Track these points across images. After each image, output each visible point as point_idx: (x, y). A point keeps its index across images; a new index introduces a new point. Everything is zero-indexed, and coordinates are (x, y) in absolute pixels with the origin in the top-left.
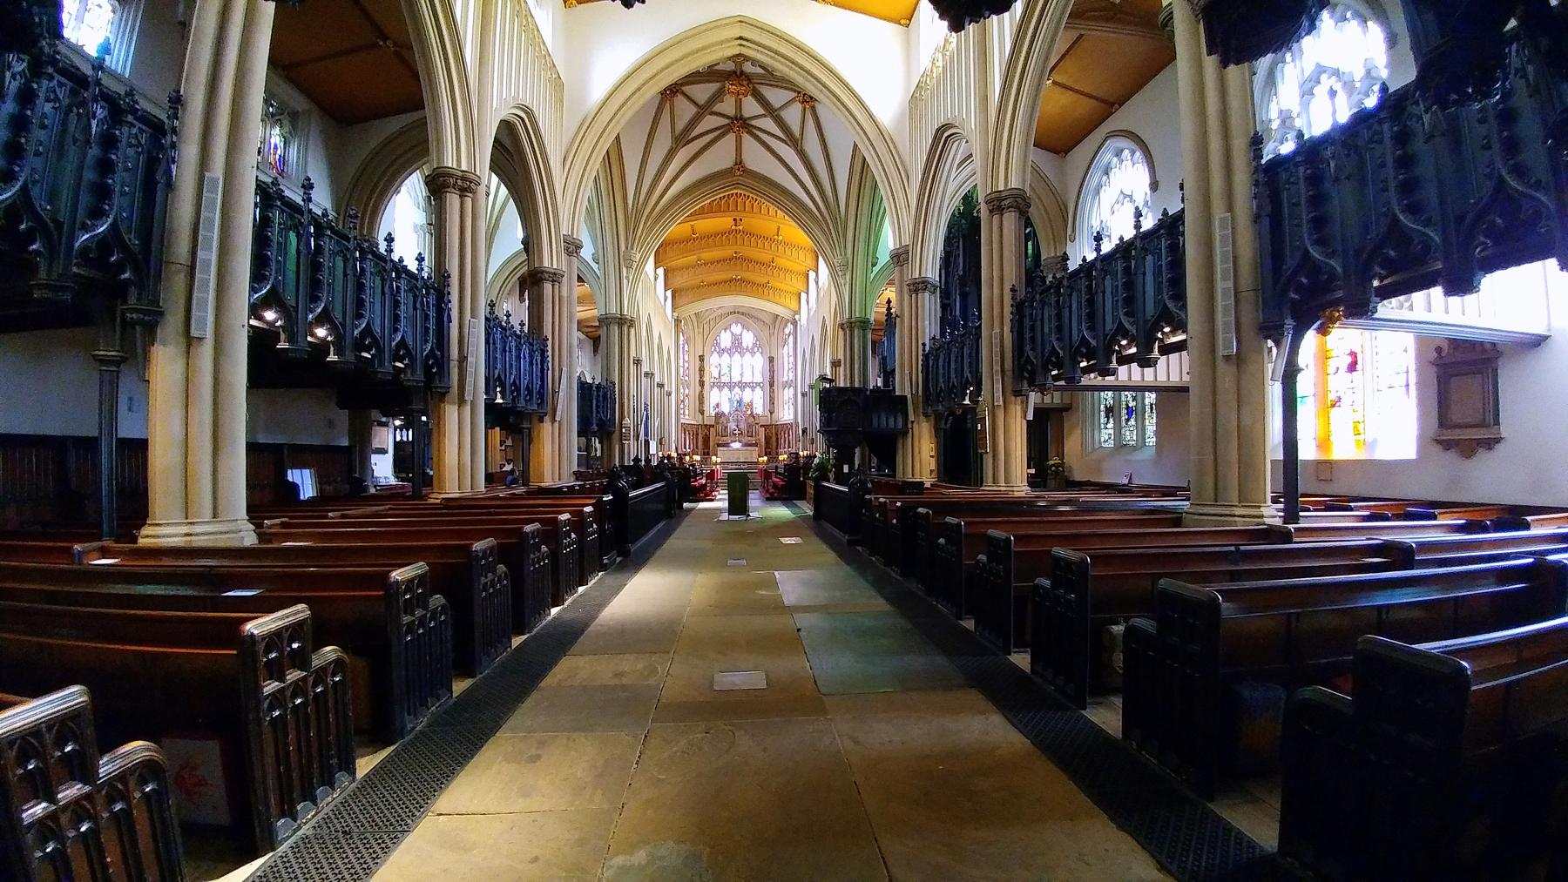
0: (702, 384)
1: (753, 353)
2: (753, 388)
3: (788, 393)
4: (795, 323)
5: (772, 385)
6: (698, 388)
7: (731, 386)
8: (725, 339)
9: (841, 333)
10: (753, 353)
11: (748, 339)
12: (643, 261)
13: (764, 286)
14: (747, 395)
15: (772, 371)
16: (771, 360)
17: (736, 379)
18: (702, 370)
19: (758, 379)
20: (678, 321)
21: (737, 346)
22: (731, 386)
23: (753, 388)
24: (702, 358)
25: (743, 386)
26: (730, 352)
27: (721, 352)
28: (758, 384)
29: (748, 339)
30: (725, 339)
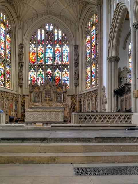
0: (21, 65)
1: (62, 46)
2: (62, 70)
5: (76, 65)
6: (18, 69)
7: (44, 66)
8: (41, 35)
10: (62, 46)
15: (77, 55)
16: (76, 47)
17: (50, 62)
18: (21, 55)
19: (65, 61)
21: (49, 39)
22: (44, 66)
23: (62, 70)
24: (21, 46)
25: (54, 67)
26: (44, 43)
27: (38, 44)
28: (66, 66)
29: (58, 34)
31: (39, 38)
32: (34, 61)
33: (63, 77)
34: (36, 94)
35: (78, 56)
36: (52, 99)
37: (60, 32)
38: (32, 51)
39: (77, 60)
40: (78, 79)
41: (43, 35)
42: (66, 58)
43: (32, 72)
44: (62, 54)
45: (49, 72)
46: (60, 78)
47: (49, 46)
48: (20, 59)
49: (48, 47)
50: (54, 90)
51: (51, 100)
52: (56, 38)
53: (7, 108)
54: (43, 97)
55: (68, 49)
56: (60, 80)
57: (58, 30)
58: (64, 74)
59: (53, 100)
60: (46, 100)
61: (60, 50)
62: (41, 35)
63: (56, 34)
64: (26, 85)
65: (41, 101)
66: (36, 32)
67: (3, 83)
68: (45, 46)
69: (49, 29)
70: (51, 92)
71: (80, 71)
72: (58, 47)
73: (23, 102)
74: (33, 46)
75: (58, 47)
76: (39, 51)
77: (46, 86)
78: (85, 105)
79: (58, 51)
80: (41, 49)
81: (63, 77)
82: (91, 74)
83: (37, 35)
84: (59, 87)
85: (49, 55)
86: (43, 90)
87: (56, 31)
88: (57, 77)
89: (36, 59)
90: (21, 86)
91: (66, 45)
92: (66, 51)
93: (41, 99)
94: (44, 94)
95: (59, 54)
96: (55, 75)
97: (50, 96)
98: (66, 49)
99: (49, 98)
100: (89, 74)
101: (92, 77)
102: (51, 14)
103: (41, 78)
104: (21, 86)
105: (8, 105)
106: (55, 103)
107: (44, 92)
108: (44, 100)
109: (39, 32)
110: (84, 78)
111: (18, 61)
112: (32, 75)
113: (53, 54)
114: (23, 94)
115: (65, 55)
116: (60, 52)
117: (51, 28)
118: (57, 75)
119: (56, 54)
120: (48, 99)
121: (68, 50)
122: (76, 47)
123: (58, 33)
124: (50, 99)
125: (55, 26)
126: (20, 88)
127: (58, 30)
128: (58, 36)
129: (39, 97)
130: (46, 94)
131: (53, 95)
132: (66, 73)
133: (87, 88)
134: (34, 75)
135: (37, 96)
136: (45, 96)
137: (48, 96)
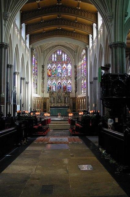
0: (43, 79)
2: (67, 80)
3: (84, 82)
4: (86, 50)
6: (41, 81)
8: (54, 57)
9: (110, 50)
10: (67, 64)
11: (65, 57)
12: (14, 16)
13: (72, 32)
14: (64, 83)
16: (75, 67)
20: (32, 50)
21: (60, 60)
24: (43, 67)
27: (52, 63)
28: (70, 77)
29: (65, 57)
30: (54, 57)
31: (53, 60)
32: (50, 75)
35: (76, 72)
37: (66, 55)
38: (49, 68)
39: (76, 75)
40: (77, 87)
41: (56, 58)
42: (69, 73)
43: (49, 82)
44: (67, 70)
45: (59, 82)
47: (59, 65)
48: (43, 75)
49: (59, 65)
50: (63, 96)
52: (63, 60)
55: (70, 67)
56: (65, 88)
57: (64, 55)
61: (66, 68)
62: (54, 58)
63: (63, 57)
64: (46, 89)
66: (52, 56)
68: (57, 65)
69: (59, 53)
71: (78, 82)
72: (65, 65)
74: (50, 65)
75: (65, 65)
76: (53, 68)
79: (64, 68)
80: (54, 67)
82: (84, 85)
83: (52, 58)
85: (59, 71)
87: (63, 55)
89: (51, 74)
91: (69, 64)
92: (69, 68)
95: (65, 70)
98: (69, 66)
100: (83, 84)
102: (60, 45)
104: (43, 92)
106: (63, 104)
109: (53, 55)
110: (80, 87)
111: (41, 76)
113: (62, 70)
115: (69, 71)
116: (66, 69)
117: (61, 53)
119: (64, 70)
121: (71, 67)
122: (75, 67)
123: (65, 56)
125: (62, 52)
127: (64, 55)
128: (64, 58)
132: (69, 83)
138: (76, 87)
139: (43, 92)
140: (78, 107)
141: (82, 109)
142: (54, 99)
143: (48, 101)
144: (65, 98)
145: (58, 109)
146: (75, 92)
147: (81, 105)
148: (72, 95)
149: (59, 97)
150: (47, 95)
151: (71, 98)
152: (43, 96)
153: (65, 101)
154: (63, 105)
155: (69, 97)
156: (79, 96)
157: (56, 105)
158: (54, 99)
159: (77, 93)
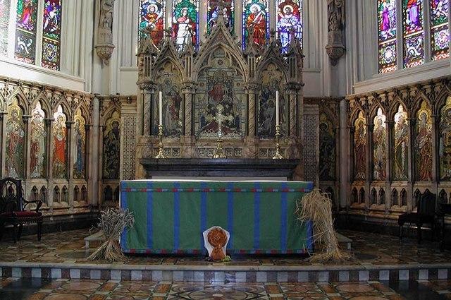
33: (280, 18)
34: (169, 94)
36: (237, 119)
40: (342, 27)
46: (264, 22)
51: (233, 126)
53: (40, 160)
54: (197, 112)
58: (281, 6)
59: (243, 126)
60: (214, 126)
65: (188, 127)
67: (29, 45)
70: (235, 87)
73: (109, 129)
77: (214, 57)
78: (379, 148)
81: (280, 18)
84: (271, 62)
86: (200, 75)
88: (252, 16)
90: (103, 55)
93: (188, 120)
94: (203, 97)
96: (248, 7)
97: (231, 106)
99: (224, 113)
101: (408, 21)
103: (188, 21)
105: (47, 147)
106: (250, 140)
107: (205, 87)
108: (203, 122)
112: (152, 10)
114: (113, 93)
118: (252, 10)
120: (220, 118)
124: (231, 118)
126: (97, 66)
129: (181, 112)
130: (214, 94)
131: (244, 102)
133: (381, 66)
134: (160, 7)
135: (170, 104)
136: (210, 107)
137: (220, 108)
138: (339, 25)
139: (104, 58)
140: (355, 169)
141: (400, 186)
142: (178, 101)
143: (130, 121)
144: (265, 96)
145: (204, 189)
146: (334, 60)
147: (380, 153)
148: (317, 80)
149: (219, 91)
150: (125, 78)
151: (309, 101)
152: (106, 79)
153: (260, 117)
154: (247, 152)
155: (295, 87)
156: (362, 89)
157: (189, 153)
158: (178, 101)
159: (347, 64)
